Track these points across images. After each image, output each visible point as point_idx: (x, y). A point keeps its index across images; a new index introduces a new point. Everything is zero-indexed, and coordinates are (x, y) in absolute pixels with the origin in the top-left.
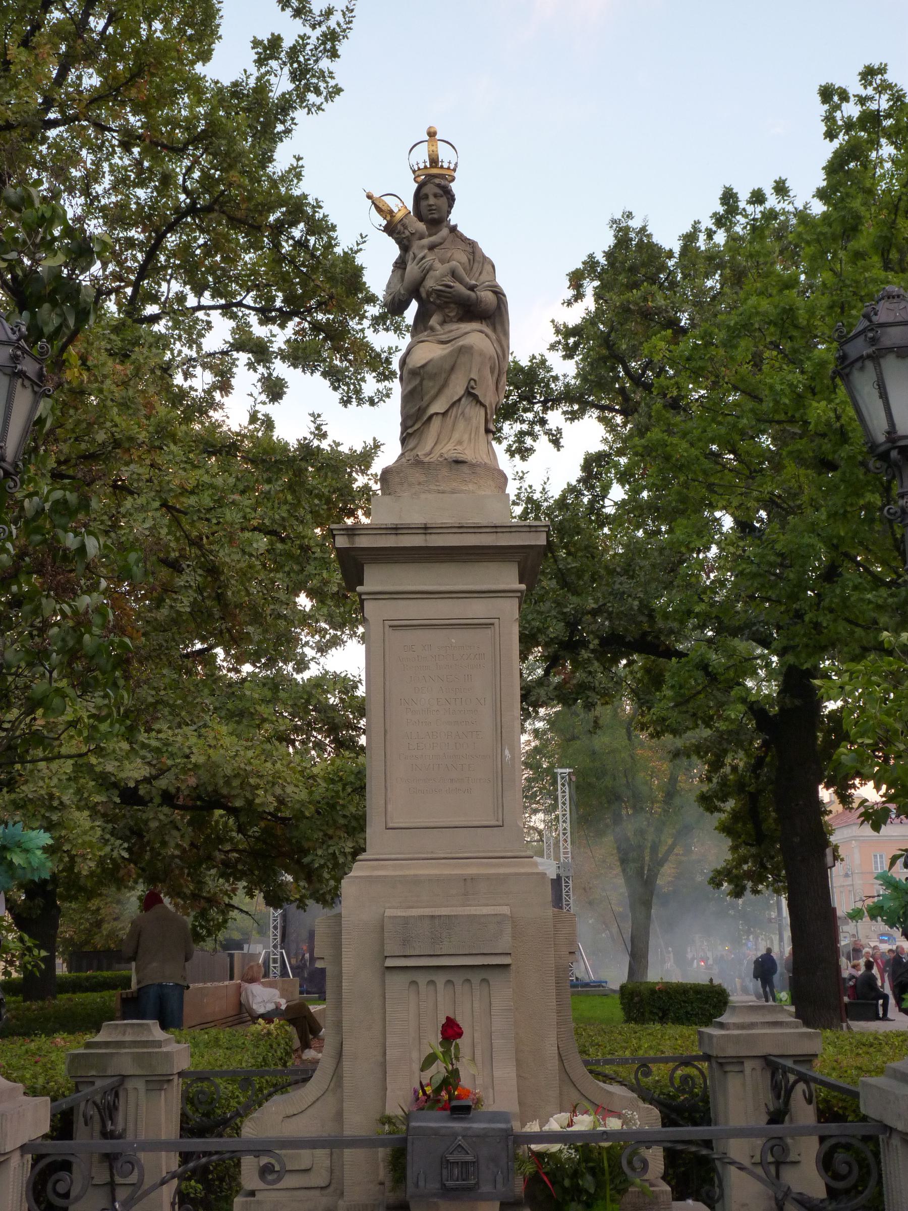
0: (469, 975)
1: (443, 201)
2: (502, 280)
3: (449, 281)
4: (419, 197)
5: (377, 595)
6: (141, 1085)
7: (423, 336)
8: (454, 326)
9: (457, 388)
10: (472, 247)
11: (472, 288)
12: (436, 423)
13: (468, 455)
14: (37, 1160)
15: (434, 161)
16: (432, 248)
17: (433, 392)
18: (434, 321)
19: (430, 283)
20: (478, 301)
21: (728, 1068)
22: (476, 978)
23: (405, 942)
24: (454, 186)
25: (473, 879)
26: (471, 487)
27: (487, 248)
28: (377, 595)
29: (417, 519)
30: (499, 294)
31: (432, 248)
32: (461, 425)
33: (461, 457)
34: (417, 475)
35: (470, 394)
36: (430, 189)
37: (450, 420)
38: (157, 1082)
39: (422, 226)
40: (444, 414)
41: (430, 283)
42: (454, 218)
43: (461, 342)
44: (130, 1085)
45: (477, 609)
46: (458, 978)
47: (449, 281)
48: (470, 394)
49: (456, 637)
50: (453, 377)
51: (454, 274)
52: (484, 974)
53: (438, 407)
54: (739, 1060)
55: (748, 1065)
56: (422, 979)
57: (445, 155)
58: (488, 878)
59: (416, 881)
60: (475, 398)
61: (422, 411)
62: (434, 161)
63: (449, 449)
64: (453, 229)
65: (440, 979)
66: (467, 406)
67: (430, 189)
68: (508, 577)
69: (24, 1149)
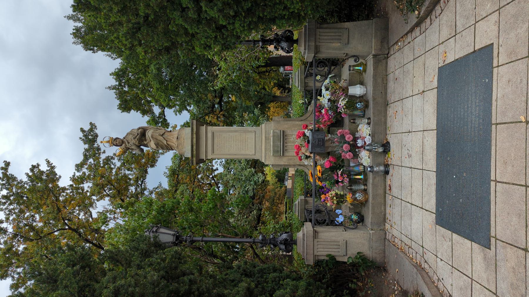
1: (118, 140)
2: (137, 127)
3: (136, 139)
4: (117, 145)
5: (206, 156)
6: (307, 206)
7: (149, 145)
9: (161, 138)
10: (127, 134)
11: (138, 134)
12: (169, 143)
13: (176, 136)
14: (316, 225)
15: (108, 142)
16: (129, 143)
18: (145, 143)
19: (137, 143)
20: (141, 133)
23: (278, 151)
24: (114, 137)
25: (266, 137)
26: (183, 136)
27: (129, 130)
28: (206, 156)
29: (190, 147)
30: (139, 128)
31: (129, 143)
32: (169, 137)
34: (180, 147)
35: (162, 135)
36: (115, 143)
38: (306, 202)
39: (123, 145)
41: (137, 143)
42: (121, 137)
43: (150, 136)
44: (306, 208)
45: (210, 135)
47: (136, 139)
48: (162, 135)
51: (134, 138)
53: (165, 142)
54: (305, 83)
55: (306, 81)
56: (285, 148)
57: (107, 139)
58: (265, 134)
60: (163, 134)
61: (165, 145)
62: (108, 142)
63: (175, 140)
64: (124, 138)
65: (285, 145)
66: (165, 136)
67: (115, 143)
68: (203, 128)
69: (313, 227)
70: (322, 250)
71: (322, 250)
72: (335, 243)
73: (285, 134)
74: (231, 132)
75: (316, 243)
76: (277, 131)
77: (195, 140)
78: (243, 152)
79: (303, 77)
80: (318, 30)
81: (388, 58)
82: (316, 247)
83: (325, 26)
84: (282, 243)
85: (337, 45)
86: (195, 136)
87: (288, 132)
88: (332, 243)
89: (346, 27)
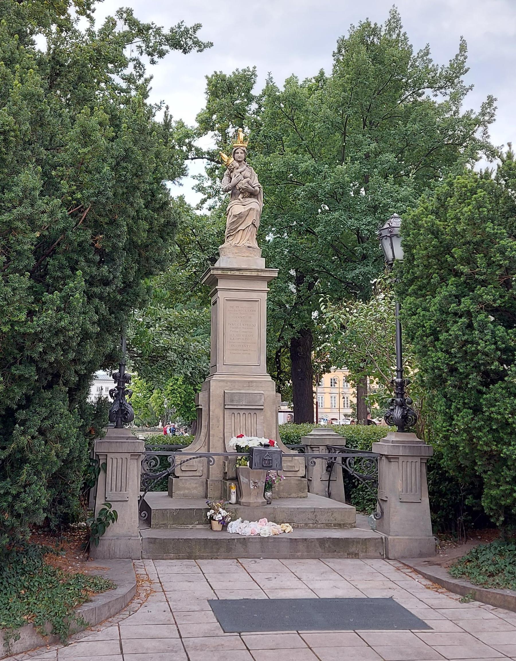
0: (250, 411)
8: (247, 199)
12: (241, 232)
17: (241, 222)
21: (314, 449)
22: (252, 412)
29: (235, 266)
33: (250, 245)
37: (245, 232)
40: (243, 230)
45: (254, 296)
46: (247, 412)
49: (245, 304)
50: (247, 218)
52: (255, 411)
56: (236, 412)
59: (234, 381)
61: (237, 228)
68: (264, 286)
70: (115, 465)
71: (115, 465)
72: (124, 485)
73: (257, 412)
74: (259, 329)
75: (124, 456)
76: (263, 400)
77: (248, 274)
78: (227, 347)
79: (328, 443)
80: (418, 460)
81: (383, 559)
82: (118, 456)
83: (424, 470)
84: (121, 406)
85: (399, 486)
86: (254, 274)
87: (260, 417)
88: (124, 480)
89: (423, 499)
